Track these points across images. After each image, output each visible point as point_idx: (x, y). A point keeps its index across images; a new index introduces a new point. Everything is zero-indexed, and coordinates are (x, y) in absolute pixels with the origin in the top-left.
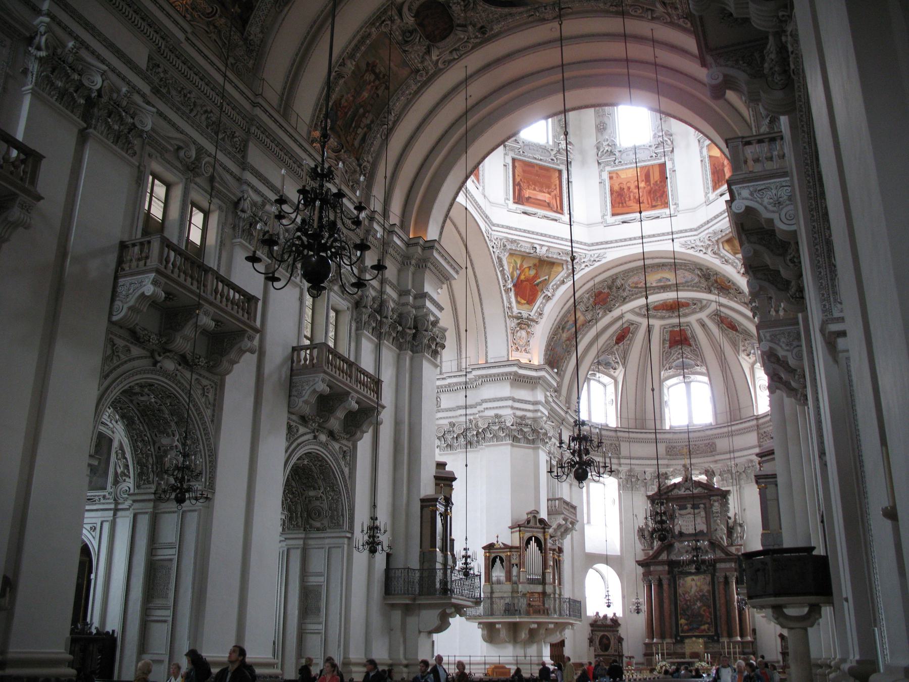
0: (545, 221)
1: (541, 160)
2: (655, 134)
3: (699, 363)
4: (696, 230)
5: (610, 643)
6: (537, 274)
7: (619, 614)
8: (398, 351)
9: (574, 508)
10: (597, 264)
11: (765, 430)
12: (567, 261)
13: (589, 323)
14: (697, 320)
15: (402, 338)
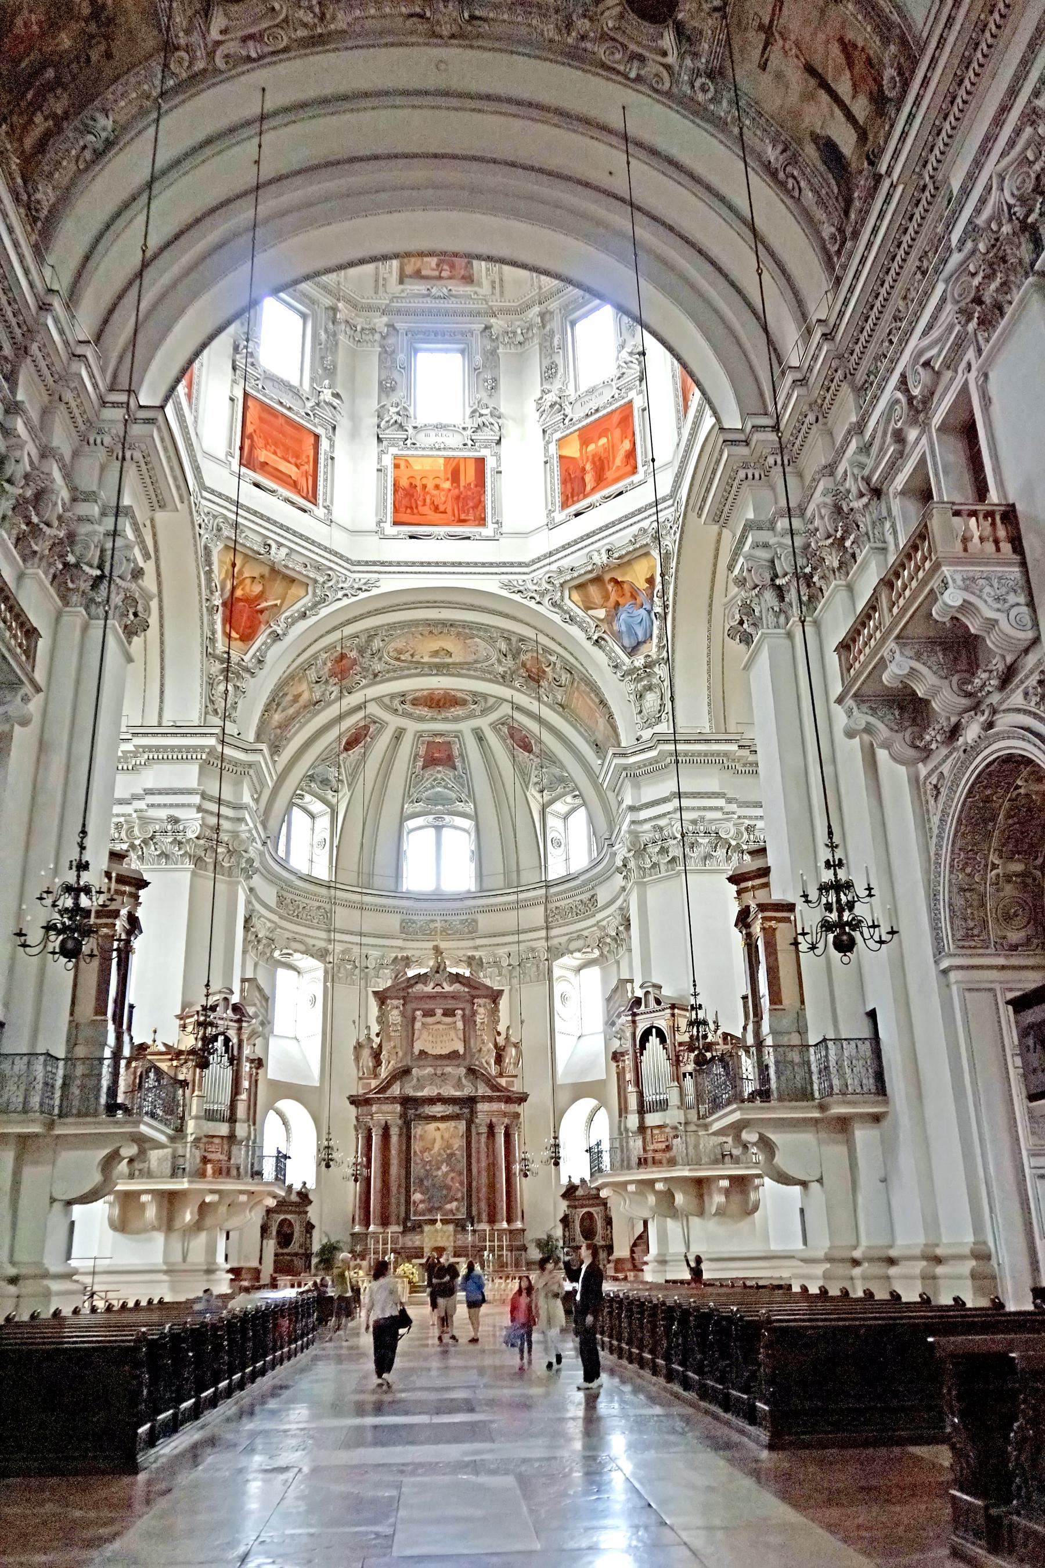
0: (288, 507)
1: (290, 409)
2: (474, 411)
3: (463, 796)
4: (527, 565)
5: (292, 1234)
6: (262, 592)
7: (311, 1185)
8: (59, 603)
9: (266, 999)
10: (363, 595)
11: (558, 904)
12: (316, 581)
13: (316, 704)
14: (473, 730)
15: (72, 582)
